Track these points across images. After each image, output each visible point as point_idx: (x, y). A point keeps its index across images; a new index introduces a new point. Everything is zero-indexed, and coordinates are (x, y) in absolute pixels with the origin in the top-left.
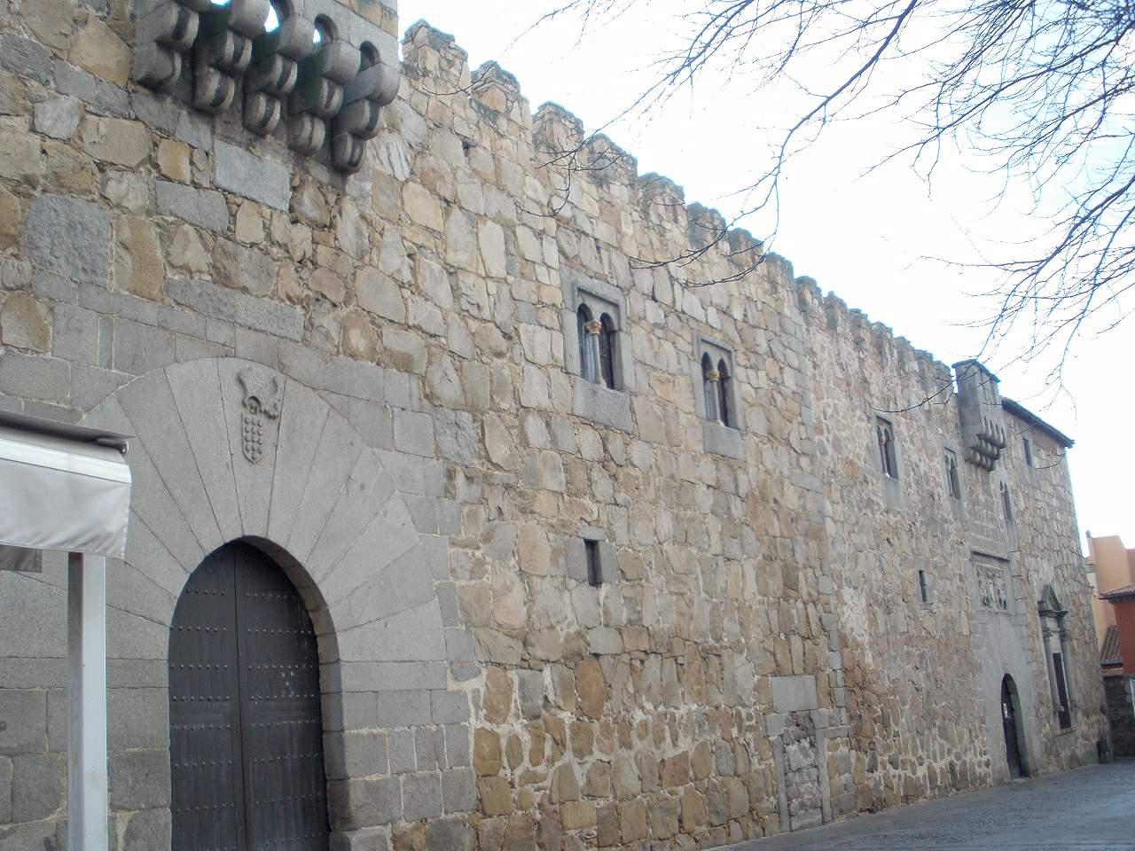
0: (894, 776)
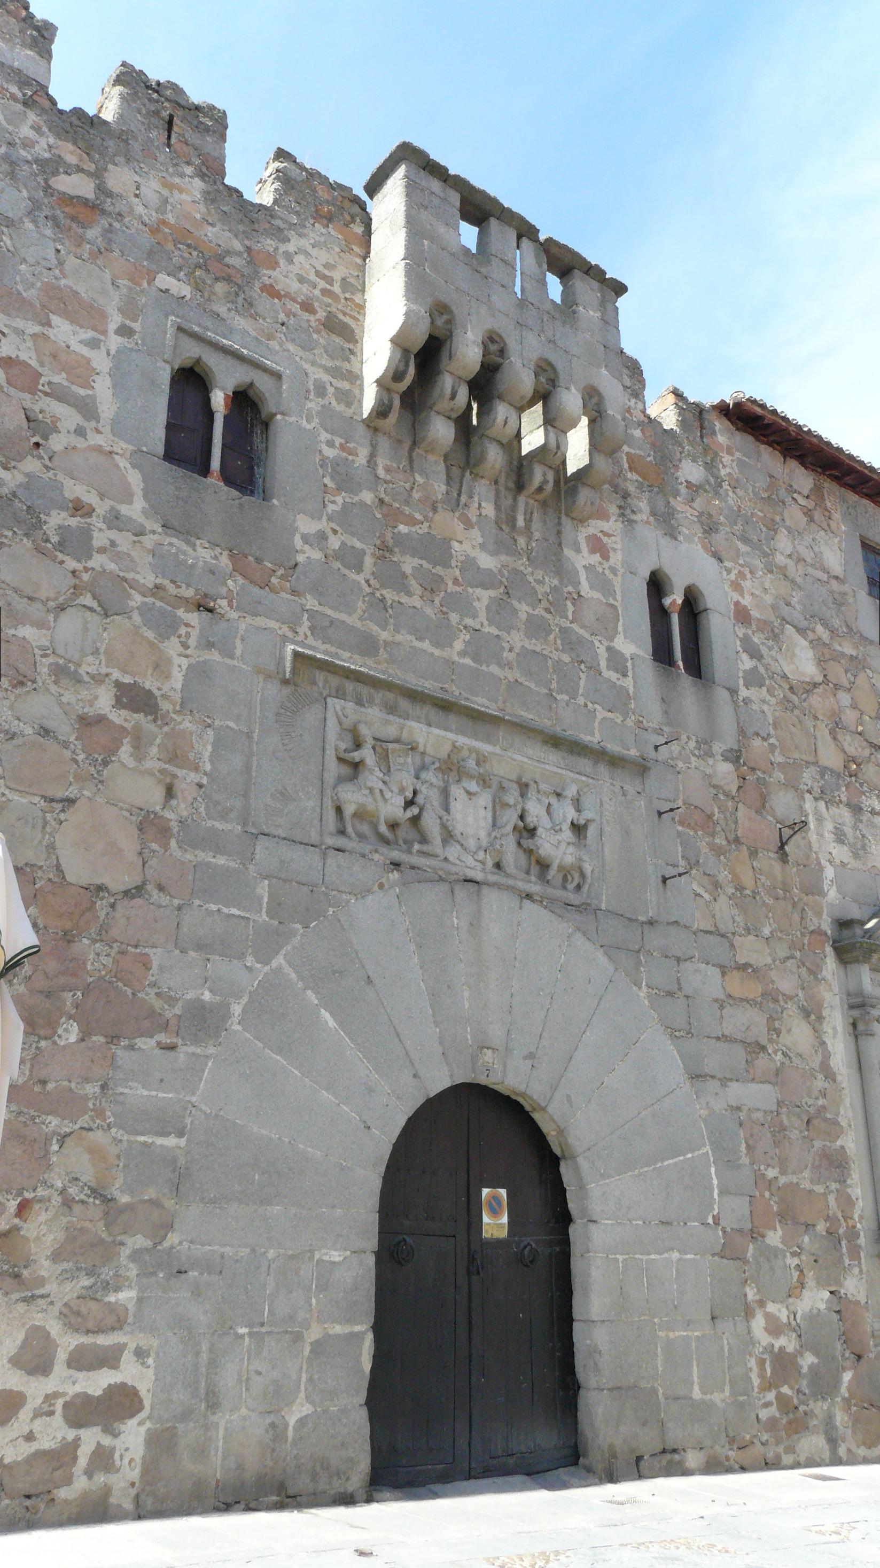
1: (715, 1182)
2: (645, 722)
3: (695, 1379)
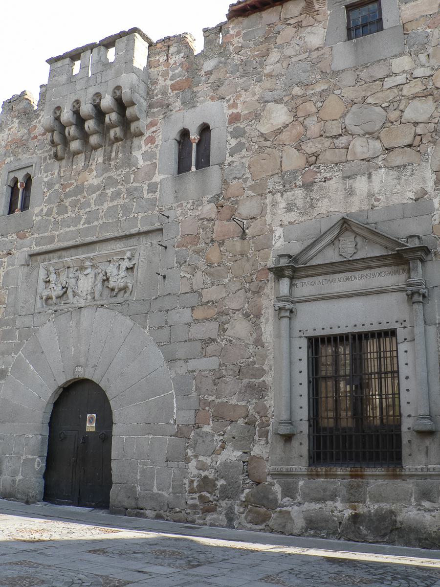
1: (175, 405)
2: (163, 208)
3: (155, 484)
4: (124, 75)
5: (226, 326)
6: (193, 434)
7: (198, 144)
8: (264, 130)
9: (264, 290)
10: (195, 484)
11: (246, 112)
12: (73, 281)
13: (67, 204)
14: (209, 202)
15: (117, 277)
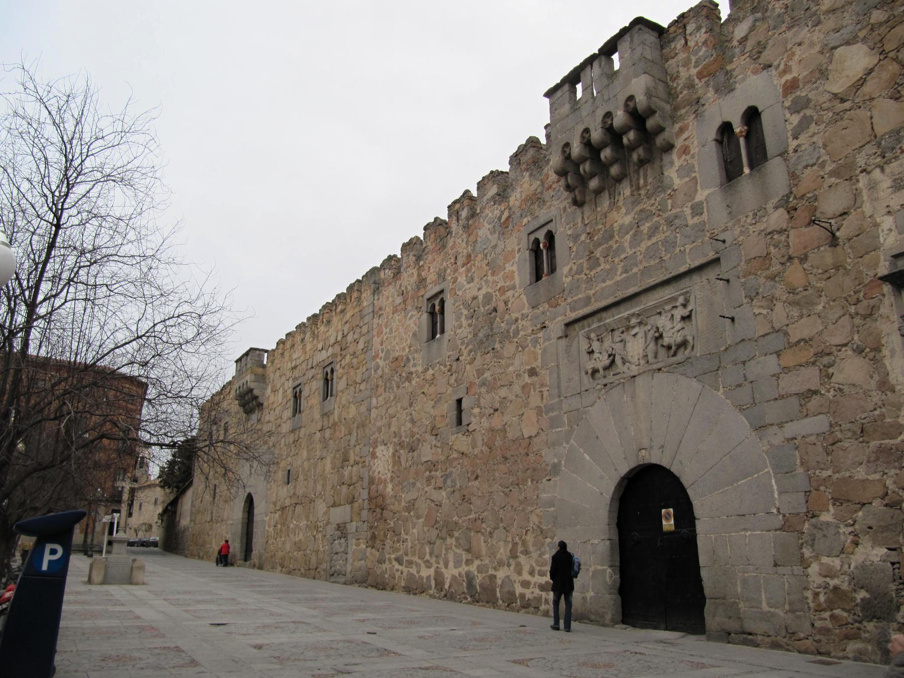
0: (398, 570)
4: (634, 81)
5: (830, 370)
6: (806, 526)
7: (747, 137)
8: (836, 89)
9: (879, 309)
10: (822, 598)
11: (807, 73)
12: (618, 347)
13: (598, 255)
14: (776, 208)
15: (672, 331)
